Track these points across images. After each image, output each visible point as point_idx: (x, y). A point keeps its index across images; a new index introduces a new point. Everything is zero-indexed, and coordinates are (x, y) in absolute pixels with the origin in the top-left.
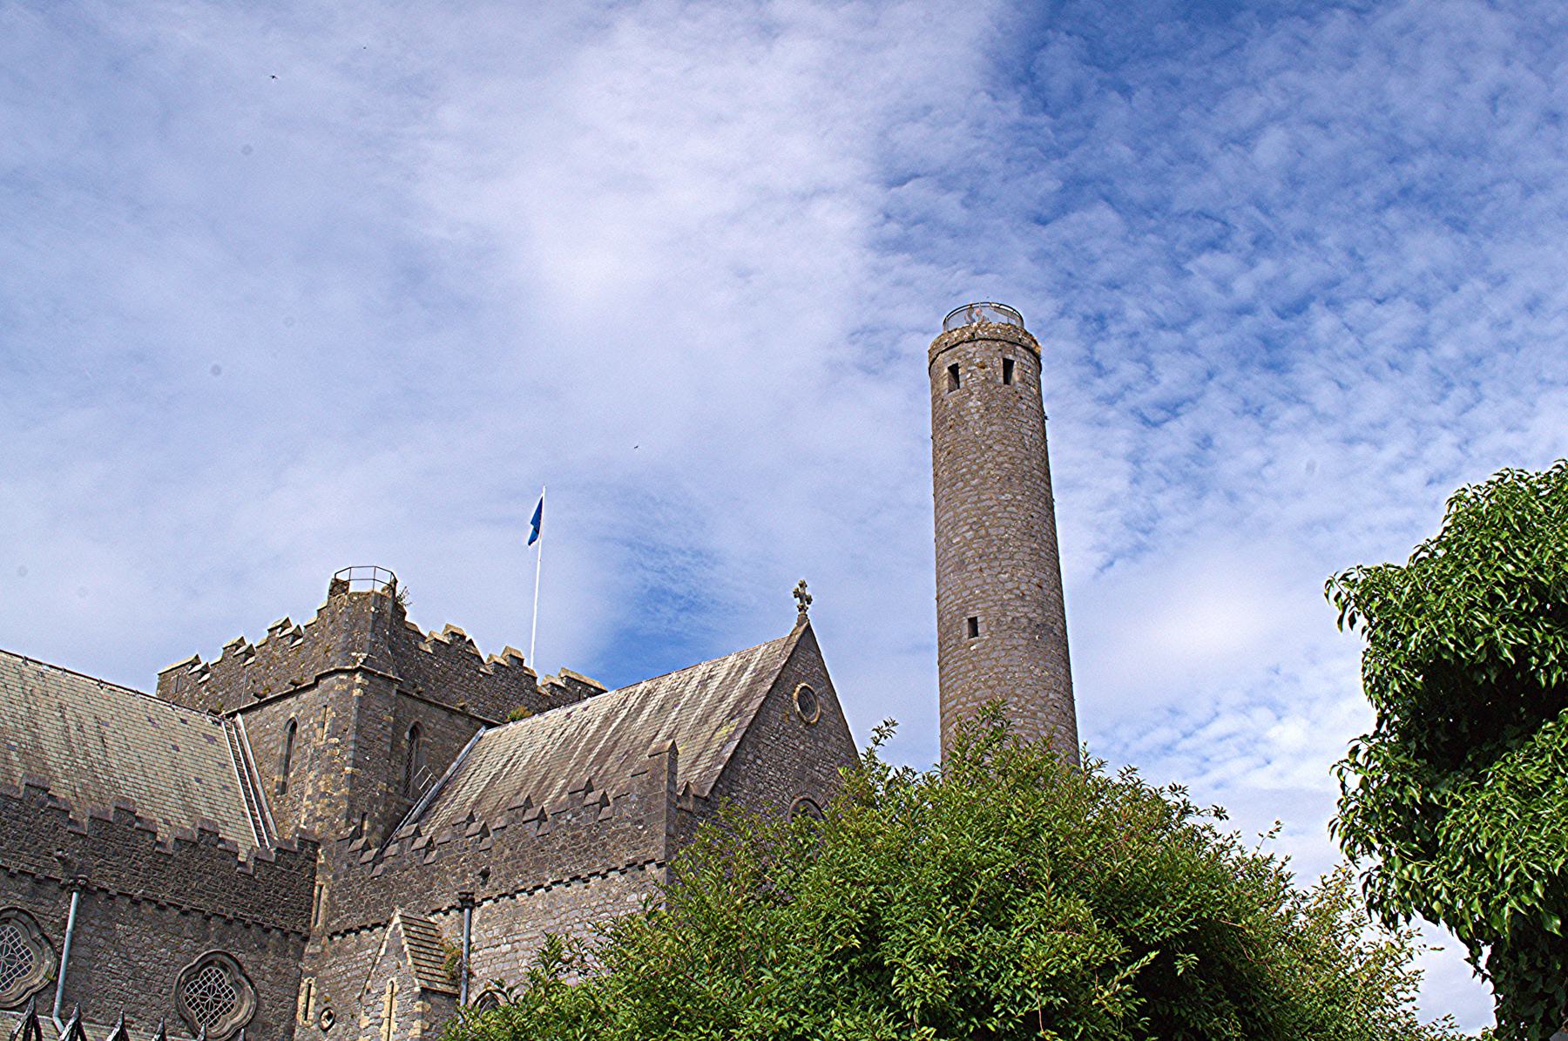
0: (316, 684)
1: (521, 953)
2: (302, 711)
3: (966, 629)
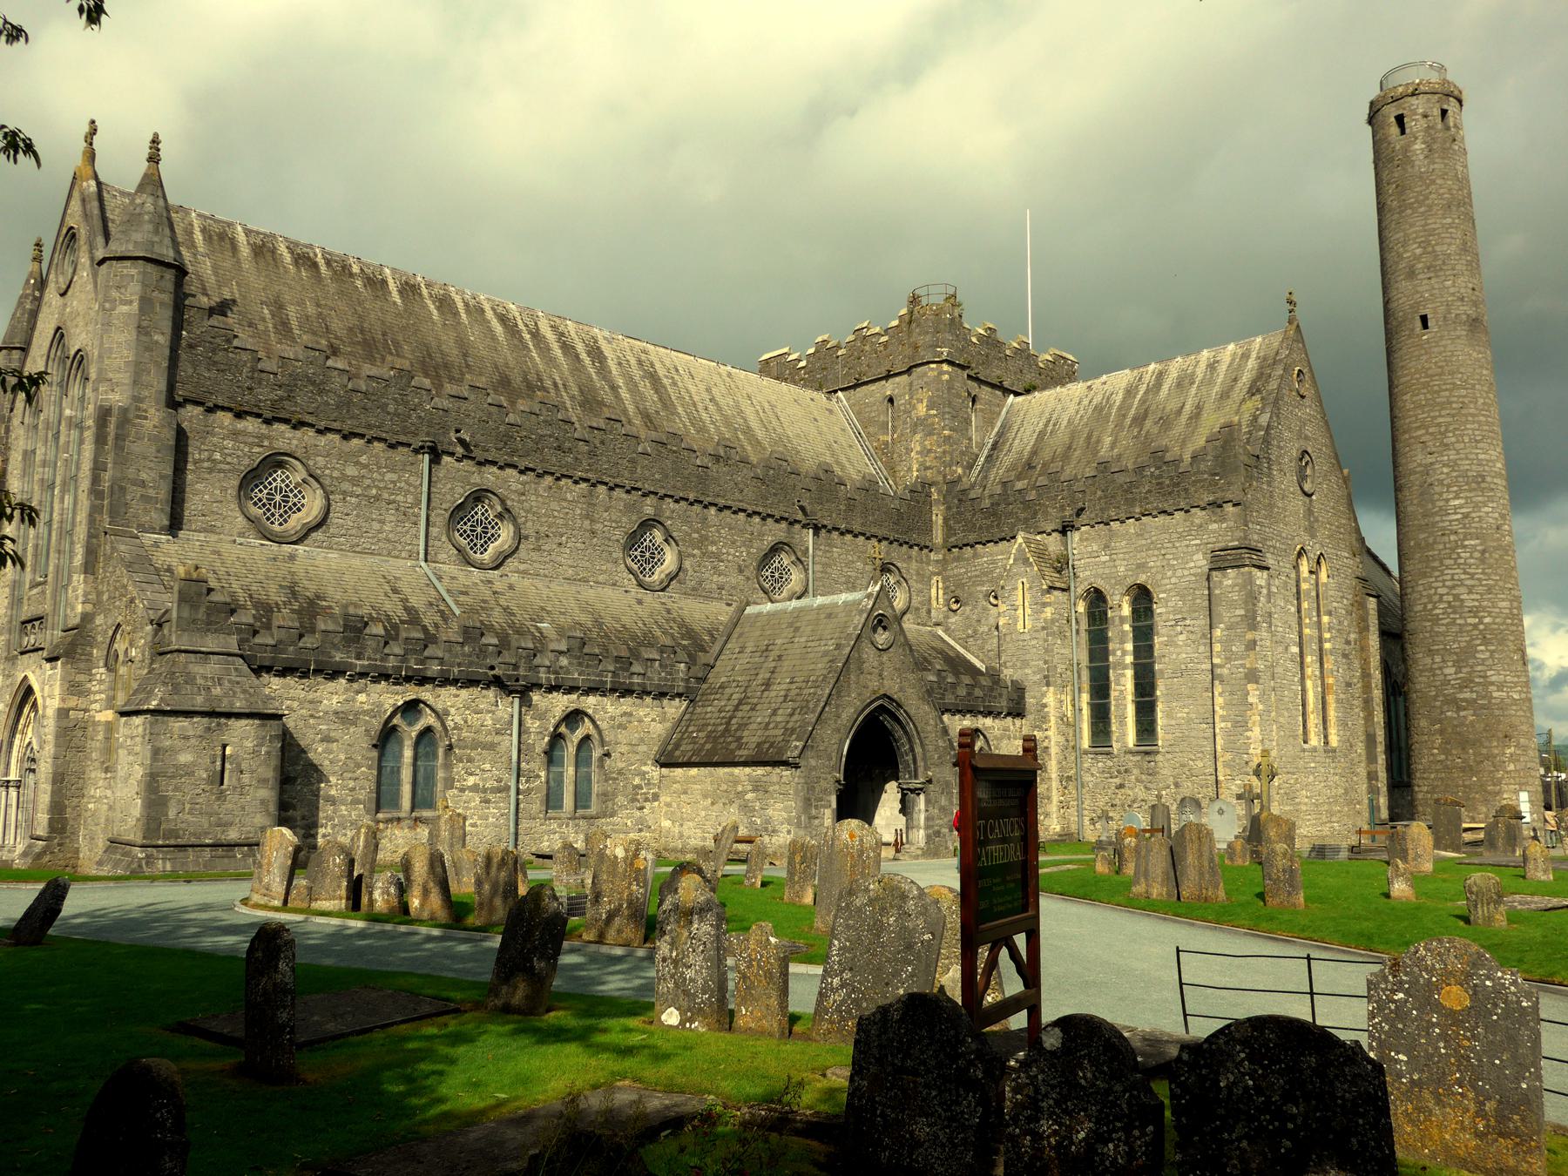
1: (1118, 563)
3: (1419, 324)
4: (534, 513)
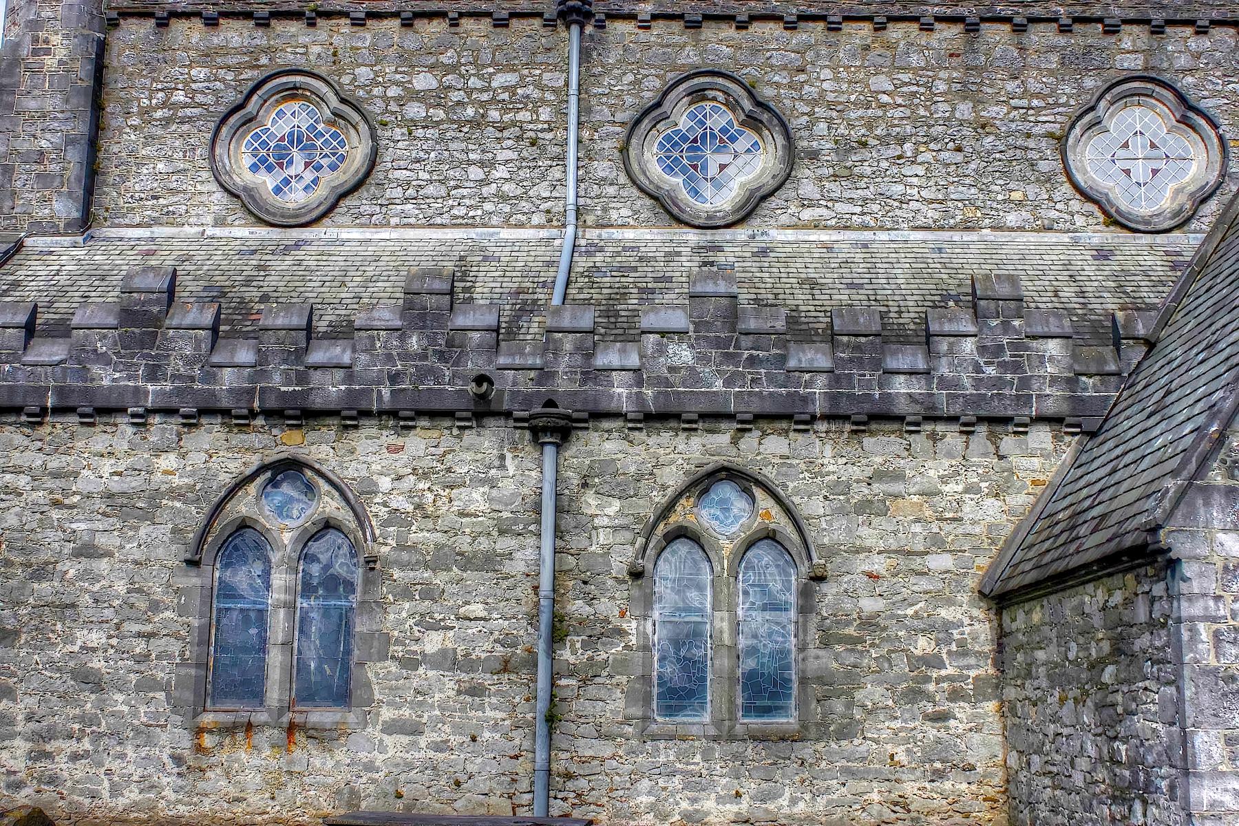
4: (830, 106)
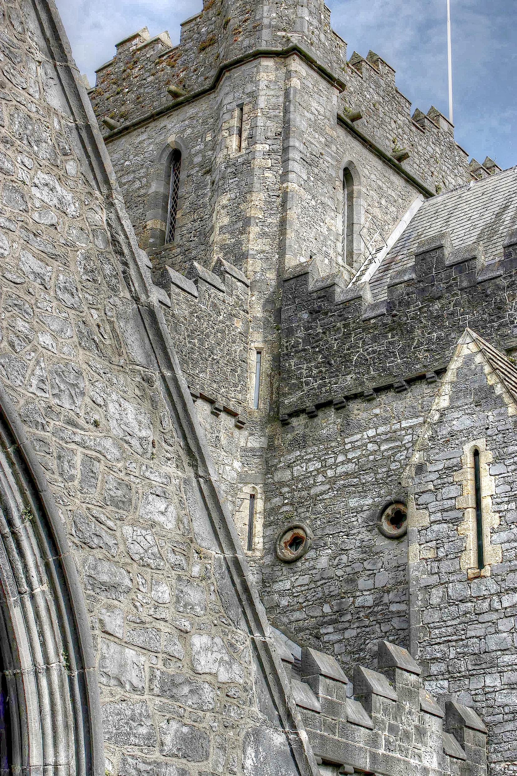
0: (213, 87)
2: (189, 131)
